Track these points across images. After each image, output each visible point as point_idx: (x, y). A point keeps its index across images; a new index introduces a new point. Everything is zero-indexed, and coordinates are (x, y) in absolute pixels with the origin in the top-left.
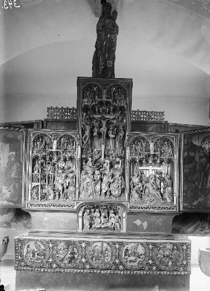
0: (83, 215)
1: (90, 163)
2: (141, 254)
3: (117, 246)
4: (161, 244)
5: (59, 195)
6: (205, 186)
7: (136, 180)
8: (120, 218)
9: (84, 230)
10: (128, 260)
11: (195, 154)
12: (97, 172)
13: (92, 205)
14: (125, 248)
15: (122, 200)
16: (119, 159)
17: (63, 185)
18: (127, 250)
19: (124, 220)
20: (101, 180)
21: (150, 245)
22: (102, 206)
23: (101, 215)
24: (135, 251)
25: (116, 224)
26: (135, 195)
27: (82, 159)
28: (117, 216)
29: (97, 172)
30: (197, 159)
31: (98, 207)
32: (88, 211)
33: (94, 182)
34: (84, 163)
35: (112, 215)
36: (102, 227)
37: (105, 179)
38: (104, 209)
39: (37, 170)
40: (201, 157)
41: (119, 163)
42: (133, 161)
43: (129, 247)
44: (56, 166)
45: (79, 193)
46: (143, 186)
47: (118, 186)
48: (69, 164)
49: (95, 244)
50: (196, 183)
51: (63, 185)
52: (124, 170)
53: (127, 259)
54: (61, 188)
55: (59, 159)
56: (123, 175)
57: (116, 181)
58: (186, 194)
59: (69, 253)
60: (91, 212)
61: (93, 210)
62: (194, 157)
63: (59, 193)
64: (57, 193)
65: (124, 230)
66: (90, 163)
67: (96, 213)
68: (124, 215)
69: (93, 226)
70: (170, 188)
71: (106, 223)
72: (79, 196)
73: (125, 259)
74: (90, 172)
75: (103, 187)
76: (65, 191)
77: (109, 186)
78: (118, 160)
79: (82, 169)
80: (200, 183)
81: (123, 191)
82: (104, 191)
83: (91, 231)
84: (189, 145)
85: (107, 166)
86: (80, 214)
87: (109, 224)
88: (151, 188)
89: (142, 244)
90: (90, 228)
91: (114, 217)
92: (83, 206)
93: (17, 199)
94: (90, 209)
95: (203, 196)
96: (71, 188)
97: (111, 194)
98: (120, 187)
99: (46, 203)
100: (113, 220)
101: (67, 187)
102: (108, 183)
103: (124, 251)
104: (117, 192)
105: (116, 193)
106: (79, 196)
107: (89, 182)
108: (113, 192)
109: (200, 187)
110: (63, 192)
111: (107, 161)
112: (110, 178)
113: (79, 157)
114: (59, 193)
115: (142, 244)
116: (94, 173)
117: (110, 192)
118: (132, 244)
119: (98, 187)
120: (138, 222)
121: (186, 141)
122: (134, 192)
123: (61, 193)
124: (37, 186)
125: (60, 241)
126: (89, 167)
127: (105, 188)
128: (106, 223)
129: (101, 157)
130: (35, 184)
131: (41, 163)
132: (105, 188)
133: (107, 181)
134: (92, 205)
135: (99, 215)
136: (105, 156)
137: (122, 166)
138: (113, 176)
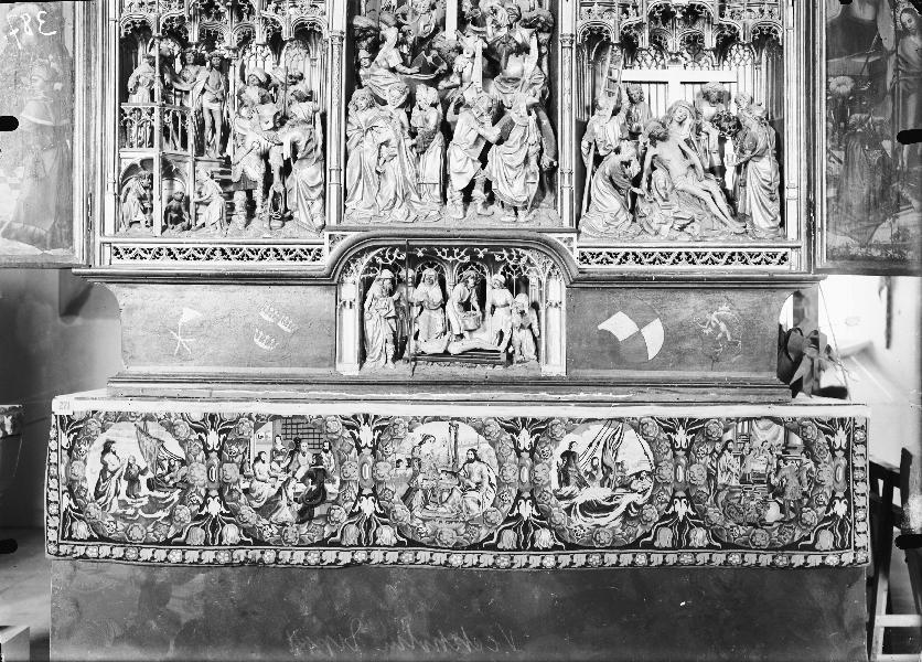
1: (390, 54)
2: (638, 475)
3: (525, 439)
4: (729, 423)
5: (251, 206)
7: (606, 129)
9: (368, 364)
10: (579, 500)
12: (426, 95)
14: (563, 446)
15: (546, 224)
16: (527, 32)
17: (265, 156)
18: (569, 455)
20: (447, 130)
21: (681, 431)
23: (445, 297)
24: (608, 461)
26: (607, 202)
27: (353, 37)
28: (522, 299)
29: (426, 95)
31: (431, 259)
32: (387, 274)
33: (410, 142)
34: (363, 54)
35: (497, 294)
36: (455, 349)
37: (465, 127)
38: (465, 267)
39: (143, 92)
41: (527, 50)
42: (595, 40)
43: (581, 441)
44: (234, 74)
45: (344, 194)
46: (642, 159)
47: (526, 161)
48: (294, 58)
49: (421, 430)
51: (265, 156)
52: (551, 82)
53: (570, 497)
54: (256, 172)
55: (246, 40)
56: (547, 105)
57: (516, 134)
59: (300, 474)
60: (396, 283)
62: (872, 27)
63: (249, 193)
64: (240, 198)
65: (555, 366)
66: (390, 54)
68: (557, 290)
69: (411, 346)
70: (766, 166)
72: (342, 209)
73: (561, 498)
74: (394, 93)
75: (454, 166)
76: (277, 186)
77: (483, 159)
78: (521, 35)
79: (353, 81)
81: (548, 179)
82: (457, 183)
83: (402, 370)
85: (470, 66)
86: (350, 291)
87: (485, 339)
88: (677, 165)
89: (639, 427)
90: (398, 356)
92: (362, 252)
93: (48, 224)
94: (394, 268)
96: (305, 173)
97: (491, 199)
98: (533, 161)
99: (190, 240)
100: (501, 320)
101: (286, 170)
102: (476, 143)
103: (556, 459)
104: (518, 185)
105: (516, 185)
106: (342, 209)
107: (386, 143)
108: (500, 188)
110: (266, 192)
111: (473, 44)
112: (488, 119)
113: (340, 24)
114: (249, 193)
115: (639, 427)
116: (410, 101)
117: (488, 185)
118: (595, 428)
119: (431, 163)
120: (620, 326)
122: (598, 185)
123: (258, 194)
124: (147, 163)
125: (259, 422)
126: (384, 72)
127: (463, 168)
129: (441, 25)
130: (134, 156)
131: (161, 56)
132: (463, 168)
133: (472, 136)
134: (402, 248)
135: (435, 294)
136: (462, 21)
137: (539, 64)
138: (499, 112)
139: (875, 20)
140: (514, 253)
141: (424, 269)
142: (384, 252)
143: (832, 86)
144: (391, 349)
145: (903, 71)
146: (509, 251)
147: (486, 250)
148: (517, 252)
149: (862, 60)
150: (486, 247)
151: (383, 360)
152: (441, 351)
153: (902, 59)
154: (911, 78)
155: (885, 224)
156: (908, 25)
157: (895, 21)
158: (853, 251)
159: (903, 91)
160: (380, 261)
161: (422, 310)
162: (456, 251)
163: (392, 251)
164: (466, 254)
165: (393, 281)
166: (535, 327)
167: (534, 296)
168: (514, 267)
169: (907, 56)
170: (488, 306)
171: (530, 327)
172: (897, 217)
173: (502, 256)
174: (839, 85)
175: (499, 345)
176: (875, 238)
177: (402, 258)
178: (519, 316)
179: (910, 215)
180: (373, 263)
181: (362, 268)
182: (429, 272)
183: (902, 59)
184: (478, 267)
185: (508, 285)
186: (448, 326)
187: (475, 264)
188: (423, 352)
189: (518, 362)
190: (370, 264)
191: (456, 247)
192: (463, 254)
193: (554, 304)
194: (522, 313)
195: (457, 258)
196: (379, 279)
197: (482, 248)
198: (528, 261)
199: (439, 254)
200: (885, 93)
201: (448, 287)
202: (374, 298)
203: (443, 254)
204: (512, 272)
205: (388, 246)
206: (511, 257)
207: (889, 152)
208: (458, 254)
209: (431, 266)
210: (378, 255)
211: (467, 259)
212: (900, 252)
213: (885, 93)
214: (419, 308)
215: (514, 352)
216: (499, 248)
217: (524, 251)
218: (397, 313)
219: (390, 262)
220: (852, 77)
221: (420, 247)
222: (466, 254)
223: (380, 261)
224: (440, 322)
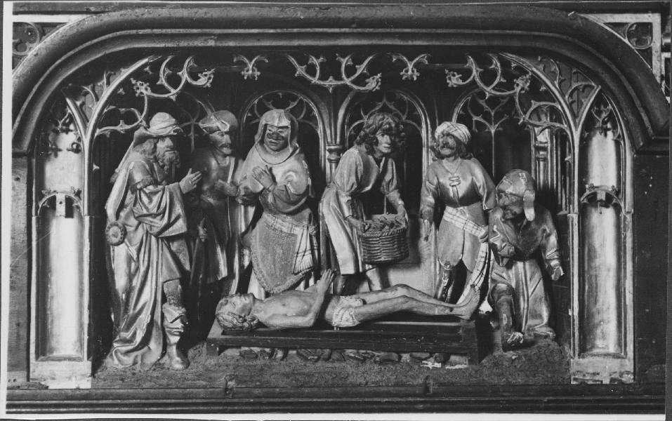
0: (100, 184)
8: (547, 200)
9: (117, 361)
13: (204, 58)
19: (604, 223)
22: (330, 69)
25: (507, 277)
28: (517, 185)
36: (344, 314)
38: (363, 103)
61: (220, 124)
67: (257, 158)
69: (230, 310)
71: (383, 269)
90: (194, 335)
91: (472, 197)
92: (92, 74)
128: (383, 269)
134: (204, 58)
140: (496, 64)
141: (263, 109)
142: (155, 67)
144: (174, 315)
146: (483, 62)
147: (423, 58)
148: (505, 64)
150: (419, 50)
151: (155, 346)
152: (308, 321)
160: (144, 90)
161: (257, 216)
162: (345, 62)
163: (176, 65)
164: (372, 70)
165: (179, 141)
166: (551, 252)
167: (546, 173)
168: (493, 101)
170: (428, 200)
171: (537, 257)
173: (466, 74)
175: (454, 299)
177: (203, 81)
178: (508, 228)
180: (124, 103)
181: (95, 110)
182: (276, 120)
184: (401, 105)
185: (473, 149)
186: (324, 260)
187: (391, 98)
188: (260, 324)
189: (507, 347)
190: (113, 98)
191: (344, 51)
192: (361, 69)
193: (601, 196)
194: (517, 220)
195: (347, 81)
196: (143, 139)
197: (412, 53)
198: (536, 82)
199: (301, 70)
201: (325, 154)
202: (130, 185)
203: (311, 70)
204: (487, 116)
205: (165, 52)
206: (488, 77)
208: (350, 71)
209: (279, 105)
210: (138, 74)
211: (373, 84)
214: (251, 210)
215: (494, 315)
216: (454, 58)
217: (525, 62)
218: (191, 224)
219: (173, 93)
221: (250, 52)
222: (372, 70)
223: (144, 90)
224: (303, 243)
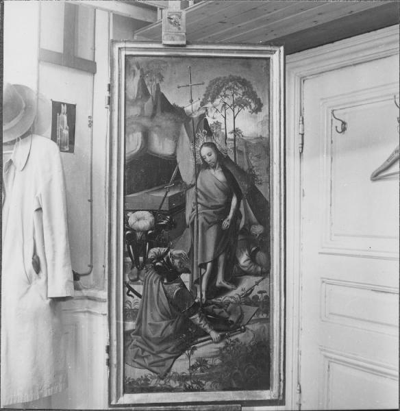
6: (223, 291)
11: (176, 147)
30: (186, 170)
40: (202, 166)
50: (185, 277)
58: (139, 323)
62: (170, 163)
80: (199, 281)
84: (149, 104)
95: (214, 335)
109: (201, 295)
121: (134, 84)
139: (174, 155)
143: (131, 221)
145: (202, 205)
149: (162, 194)
153: (201, 192)
154: (210, 212)
155: (183, 356)
156: (208, 159)
157: (195, 155)
158: (153, 383)
159: (203, 224)
169: (206, 188)
172: (195, 348)
174: (139, 220)
176: (174, 369)
179: (209, 346)
183: (201, 192)
200: (185, 226)
207: (188, 285)
212: (199, 383)
213: (185, 226)
220: (149, 211)
